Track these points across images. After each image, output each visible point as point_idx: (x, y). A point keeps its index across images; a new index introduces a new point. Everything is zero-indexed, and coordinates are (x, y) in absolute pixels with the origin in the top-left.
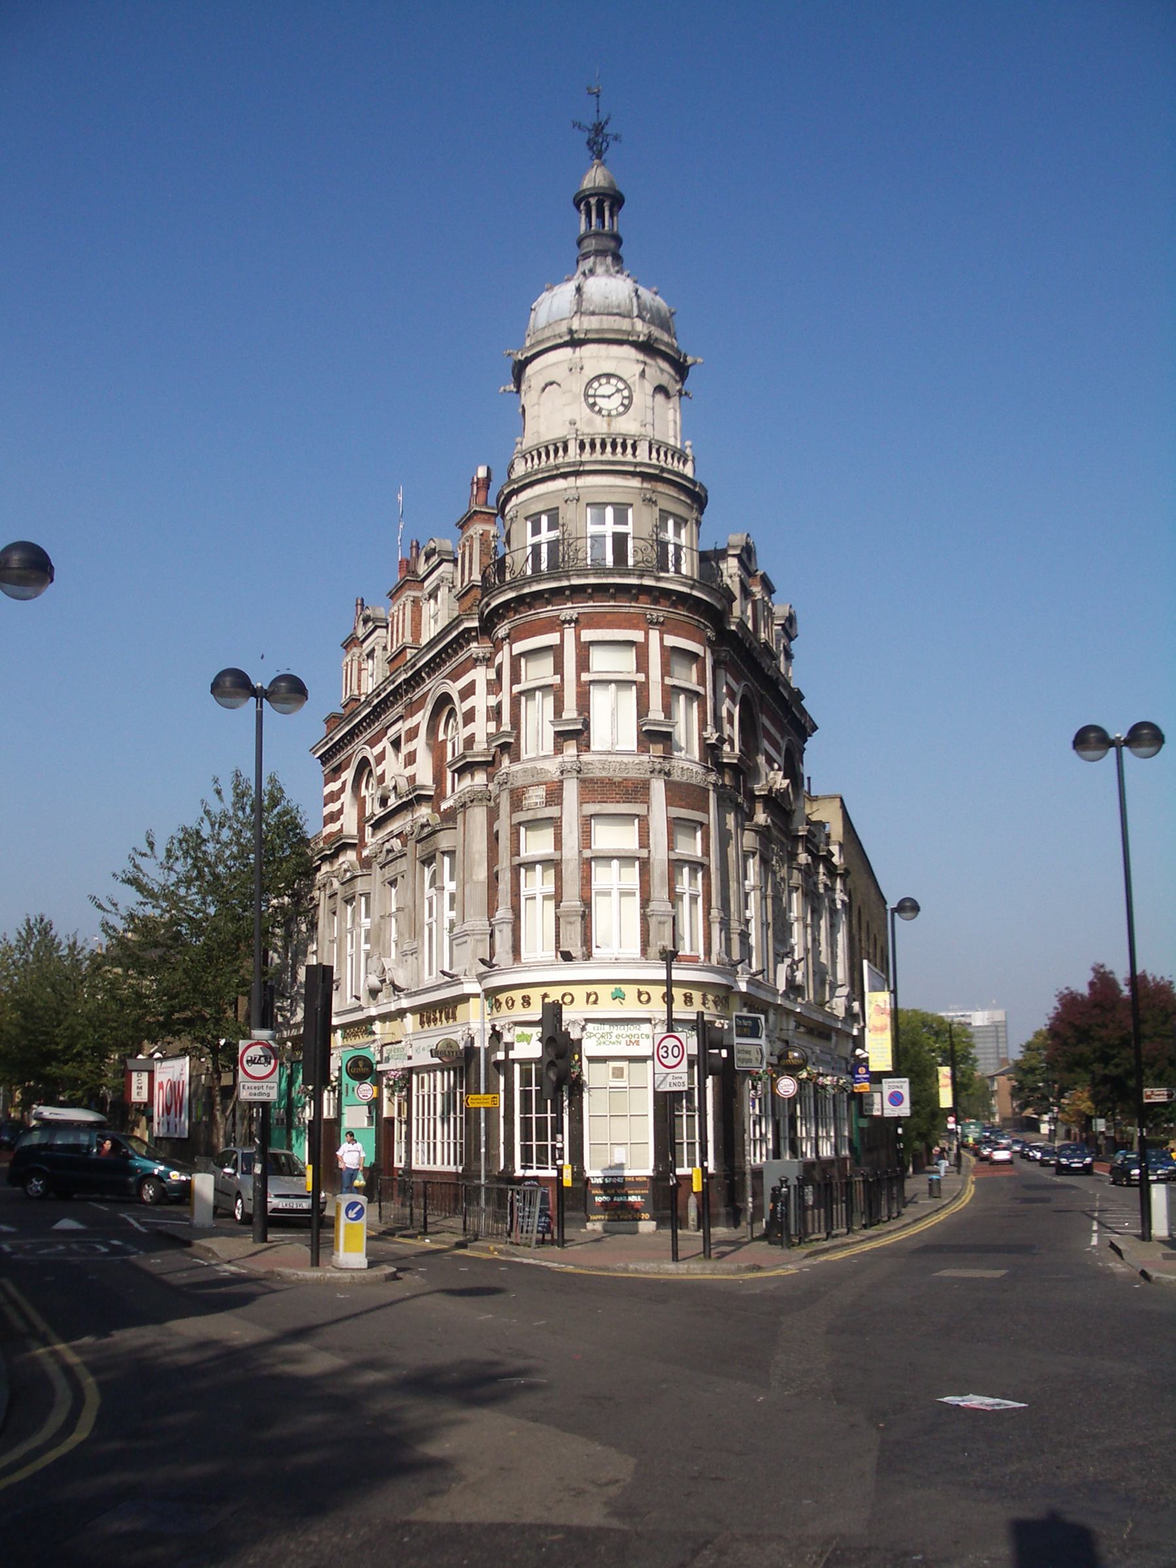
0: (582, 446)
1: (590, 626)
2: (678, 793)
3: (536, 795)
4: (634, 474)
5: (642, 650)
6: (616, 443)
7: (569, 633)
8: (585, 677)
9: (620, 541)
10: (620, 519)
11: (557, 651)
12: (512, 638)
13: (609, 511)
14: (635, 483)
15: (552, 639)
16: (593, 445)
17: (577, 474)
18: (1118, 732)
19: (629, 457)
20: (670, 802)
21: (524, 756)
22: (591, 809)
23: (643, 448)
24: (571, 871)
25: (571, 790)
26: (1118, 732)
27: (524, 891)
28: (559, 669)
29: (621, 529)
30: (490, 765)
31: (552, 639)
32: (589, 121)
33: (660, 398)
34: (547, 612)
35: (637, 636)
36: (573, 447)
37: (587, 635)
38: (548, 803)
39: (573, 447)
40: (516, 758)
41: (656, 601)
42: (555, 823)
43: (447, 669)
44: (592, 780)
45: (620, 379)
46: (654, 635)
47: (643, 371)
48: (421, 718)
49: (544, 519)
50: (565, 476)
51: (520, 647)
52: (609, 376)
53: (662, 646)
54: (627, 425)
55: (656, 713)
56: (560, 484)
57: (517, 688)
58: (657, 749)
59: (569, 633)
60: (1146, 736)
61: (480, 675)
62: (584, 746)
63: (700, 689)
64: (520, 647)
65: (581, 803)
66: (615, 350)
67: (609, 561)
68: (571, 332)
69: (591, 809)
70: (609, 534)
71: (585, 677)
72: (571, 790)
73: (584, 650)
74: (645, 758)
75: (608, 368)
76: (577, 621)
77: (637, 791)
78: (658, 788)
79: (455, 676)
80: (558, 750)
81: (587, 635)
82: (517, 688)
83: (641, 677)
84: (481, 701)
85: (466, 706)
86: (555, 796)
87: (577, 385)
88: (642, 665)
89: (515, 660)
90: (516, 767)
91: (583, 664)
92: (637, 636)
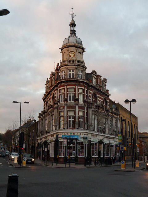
0: (68, 62)
1: (69, 86)
2: (79, 107)
3: (62, 108)
4: (74, 65)
5: (75, 89)
6: (72, 61)
7: (66, 87)
8: (68, 92)
9: (73, 74)
10: (73, 71)
11: (64, 89)
12: (59, 87)
13: (71, 71)
14: (75, 66)
15: (64, 87)
16: (69, 61)
17: (67, 65)
18: (130, 100)
19: (74, 63)
20: (78, 108)
21: (61, 103)
22: (68, 110)
23: (76, 61)
24: (66, 118)
25: (66, 107)
26: (130, 100)
27: (61, 120)
28: (64, 91)
29: (73, 73)
30: (57, 103)
31: (64, 87)
32: (72, 13)
33: (79, 54)
34: (63, 84)
35: (75, 87)
36: (67, 62)
37: (68, 87)
38: (63, 109)
39: (67, 62)
40: (60, 103)
41: (77, 82)
42: (64, 111)
43: (54, 90)
44: (68, 106)
45: (73, 52)
46: (77, 87)
47: (77, 51)
48: (52, 96)
49: (63, 72)
50: (66, 66)
51: (60, 88)
52: (72, 51)
53: (78, 88)
54: (74, 58)
55: (77, 97)
56: (65, 67)
57: (60, 94)
58: (77, 102)
59: (66, 87)
60: (134, 101)
61: (56, 91)
62: (67, 102)
63: (84, 93)
64: (60, 88)
65: (67, 109)
66: (73, 48)
67: (71, 77)
68: (67, 46)
69: (68, 110)
70: (71, 73)
71: (68, 92)
72: (66, 107)
73: (67, 89)
74: (75, 103)
75: (72, 50)
76: (67, 85)
77: (74, 107)
78: (77, 107)
79: (54, 91)
80: (64, 102)
81: (68, 87)
82: (60, 94)
83: (75, 92)
84: (56, 95)
85: (55, 95)
86: (64, 108)
87: (68, 53)
88: (75, 91)
89: (60, 90)
90: (59, 104)
91: (67, 91)
92: (75, 87)
